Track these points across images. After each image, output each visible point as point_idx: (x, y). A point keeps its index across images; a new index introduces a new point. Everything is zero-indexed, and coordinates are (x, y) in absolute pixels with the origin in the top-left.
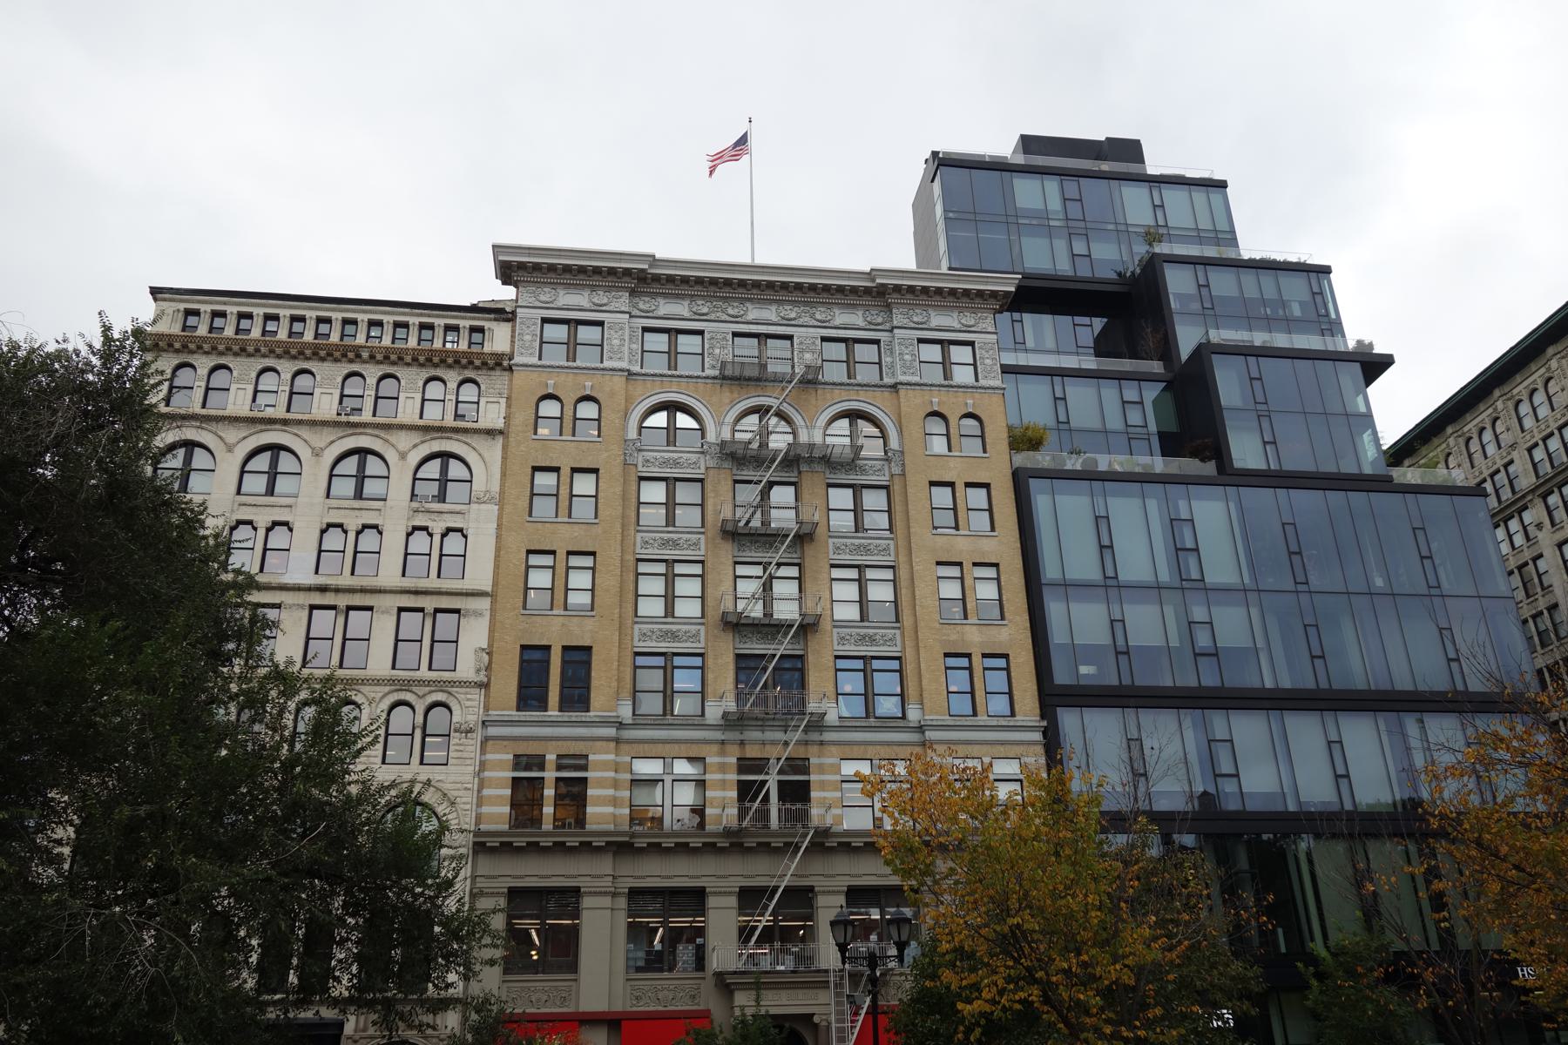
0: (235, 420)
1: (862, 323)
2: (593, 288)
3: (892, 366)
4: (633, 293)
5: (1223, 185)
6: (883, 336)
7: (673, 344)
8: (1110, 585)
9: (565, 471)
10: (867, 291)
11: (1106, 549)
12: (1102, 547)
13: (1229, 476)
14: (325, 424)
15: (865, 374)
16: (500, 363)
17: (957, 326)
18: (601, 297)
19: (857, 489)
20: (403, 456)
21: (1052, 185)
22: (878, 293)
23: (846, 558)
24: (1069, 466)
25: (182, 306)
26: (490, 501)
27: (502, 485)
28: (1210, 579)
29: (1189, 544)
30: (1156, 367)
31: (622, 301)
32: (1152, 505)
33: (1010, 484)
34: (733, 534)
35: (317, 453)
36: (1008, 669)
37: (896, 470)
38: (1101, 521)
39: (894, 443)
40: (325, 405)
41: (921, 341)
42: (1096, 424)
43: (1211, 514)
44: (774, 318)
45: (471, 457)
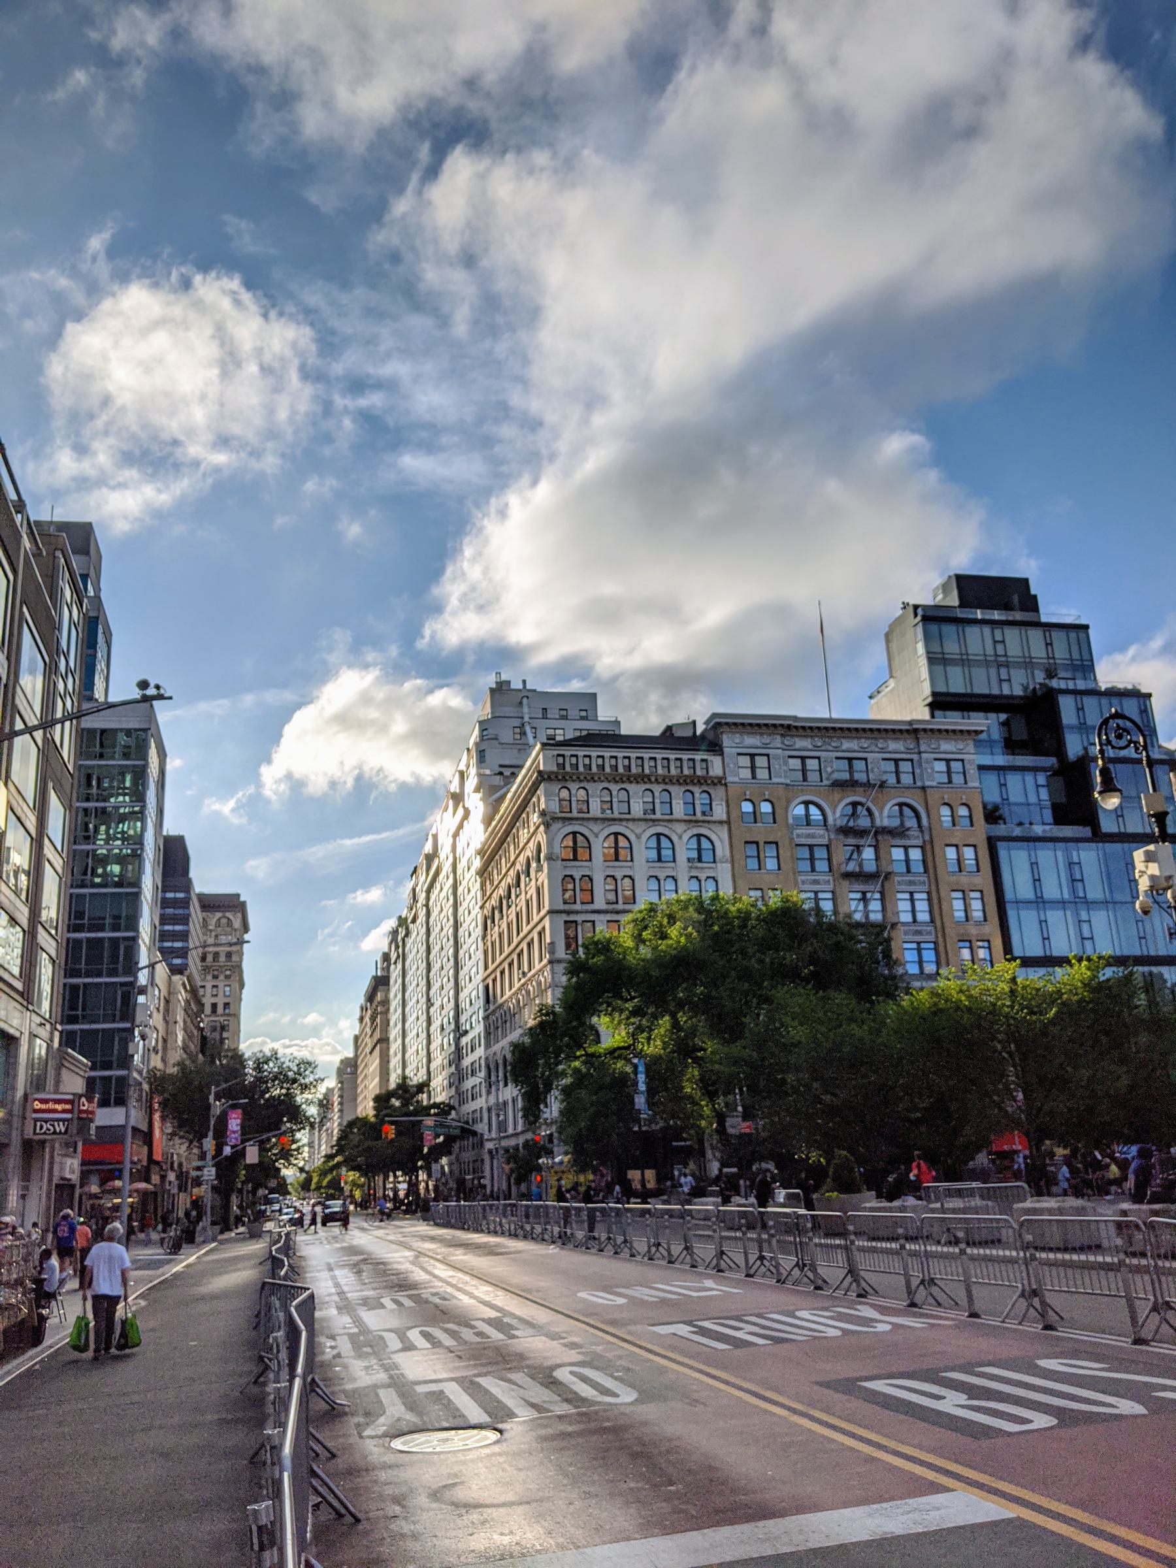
0: (596, 819)
1: (902, 749)
2: (762, 734)
3: (922, 774)
4: (782, 735)
5: (1086, 627)
6: (915, 757)
7: (804, 764)
8: (1040, 902)
9: (761, 844)
10: (907, 731)
11: (1037, 881)
12: (1035, 880)
13: (1098, 836)
14: (639, 820)
15: (906, 779)
16: (720, 781)
17: (954, 750)
18: (766, 739)
19: (906, 848)
20: (680, 837)
21: (987, 630)
22: (912, 732)
23: (904, 888)
24: (1014, 834)
25: (556, 753)
26: (726, 861)
27: (732, 852)
28: (1090, 896)
29: (1078, 877)
30: (1052, 761)
31: (777, 741)
32: (1059, 854)
33: (986, 846)
34: (848, 876)
35: (638, 837)
36: (989, 948)
37: (927, 837)
38: (1034, 865)
39: (925, 822)
40: (637, 809)
41: (936, 759)
42: (1022, 800)
43: (1089, 857)
44: (856, 748)
45: (713, 837)
